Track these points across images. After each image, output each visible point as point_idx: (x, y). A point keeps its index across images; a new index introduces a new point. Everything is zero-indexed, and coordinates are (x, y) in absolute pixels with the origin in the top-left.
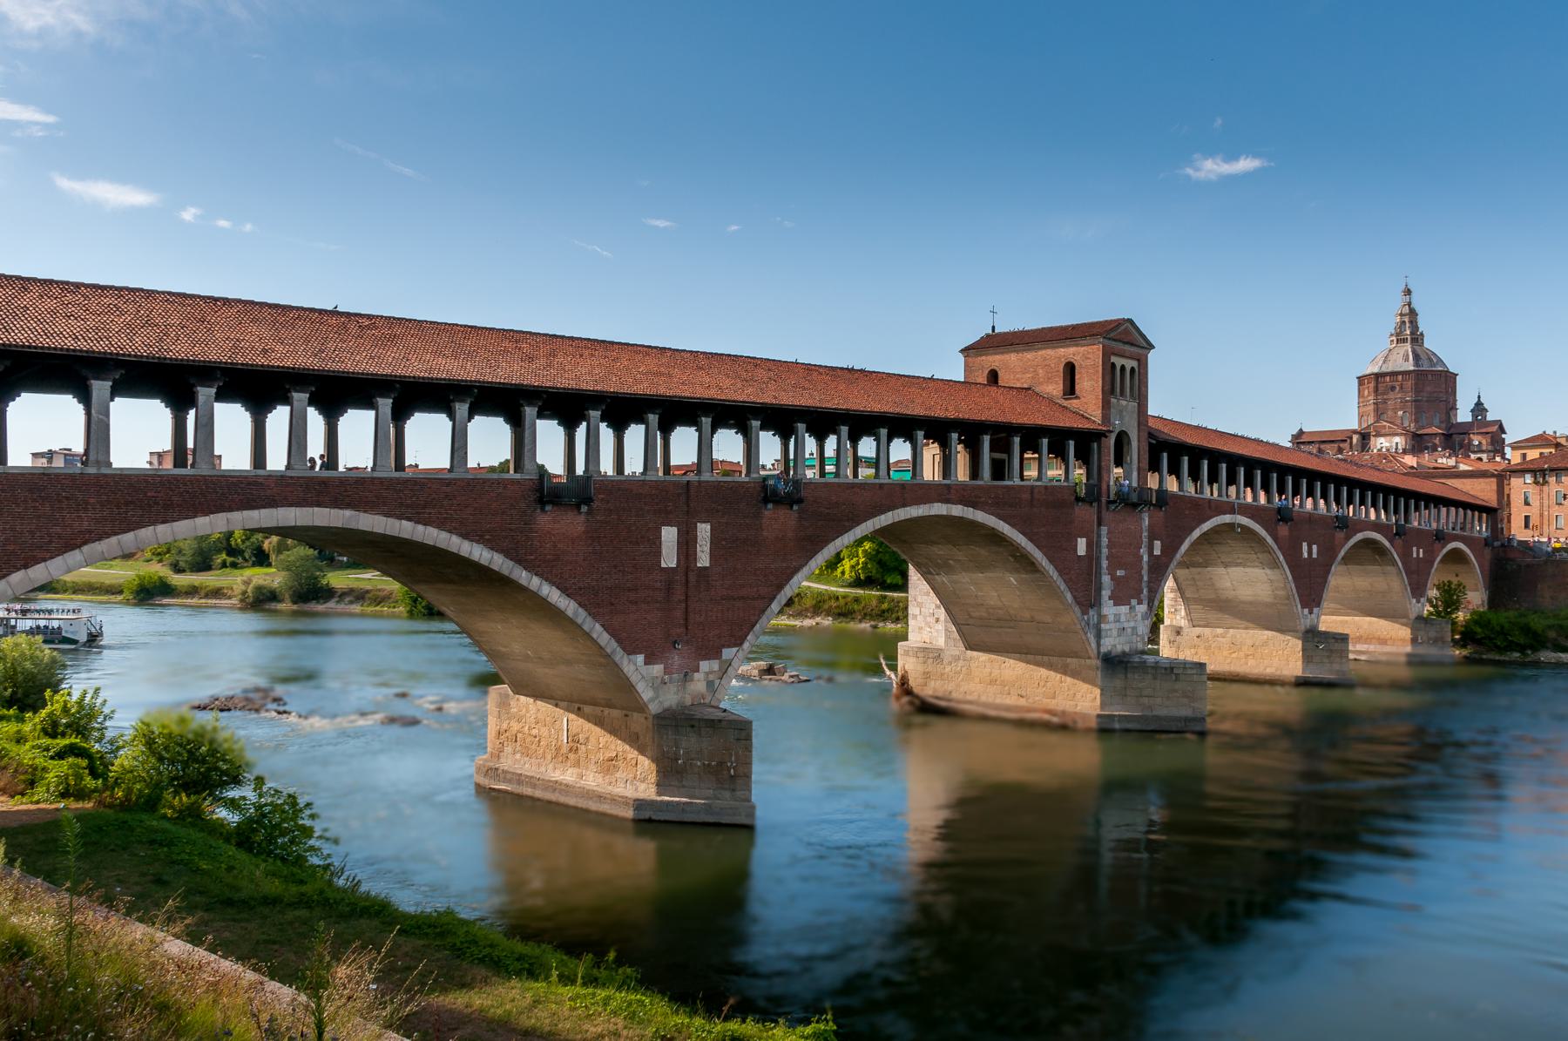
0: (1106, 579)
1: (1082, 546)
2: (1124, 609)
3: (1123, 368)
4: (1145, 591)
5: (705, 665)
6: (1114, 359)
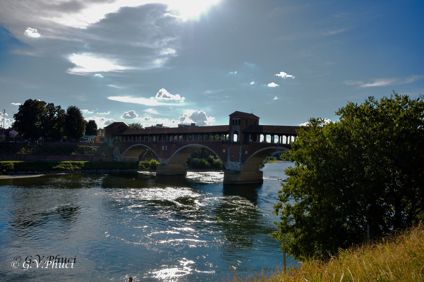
0: (229, 157)
1: (224, 151)
2: (234, 163)
3: (236, 120)
4: (240, 160)
5: (166, 160)
6: (233, 119)
